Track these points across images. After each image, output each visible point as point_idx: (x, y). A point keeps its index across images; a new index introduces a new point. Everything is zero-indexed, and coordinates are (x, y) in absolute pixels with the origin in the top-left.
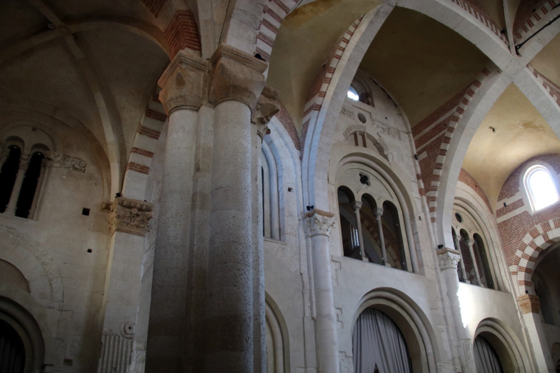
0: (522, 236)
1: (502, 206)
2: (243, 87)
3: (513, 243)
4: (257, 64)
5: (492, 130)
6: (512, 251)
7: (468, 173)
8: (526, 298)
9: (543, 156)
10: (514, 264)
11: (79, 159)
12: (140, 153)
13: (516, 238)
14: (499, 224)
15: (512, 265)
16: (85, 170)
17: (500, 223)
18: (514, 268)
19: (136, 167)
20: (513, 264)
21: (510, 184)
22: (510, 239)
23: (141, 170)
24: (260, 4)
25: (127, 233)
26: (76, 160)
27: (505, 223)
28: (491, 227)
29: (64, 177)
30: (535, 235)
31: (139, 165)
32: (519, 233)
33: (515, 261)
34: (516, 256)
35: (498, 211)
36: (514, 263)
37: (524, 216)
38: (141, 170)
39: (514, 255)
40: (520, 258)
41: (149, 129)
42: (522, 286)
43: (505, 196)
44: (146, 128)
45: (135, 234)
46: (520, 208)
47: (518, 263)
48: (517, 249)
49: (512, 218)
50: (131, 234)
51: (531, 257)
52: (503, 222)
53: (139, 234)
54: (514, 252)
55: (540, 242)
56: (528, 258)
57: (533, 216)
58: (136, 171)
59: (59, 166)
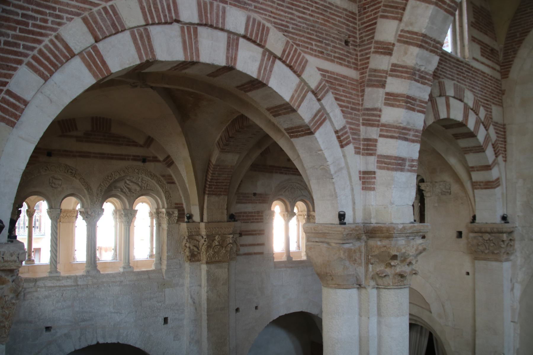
2: (323, 273)
4: (334, 233)
11: (444, 181)
12: (478, 170)
16: (450, 192)
19: (480, 185)
23: (486, 187)
24: (319, 151)
25: (484, 260)
26: (442, 183)
29: (436, 205)
31: (482, 182)
38: (486, 187)
41: (469, 148)
44: (466, 148)
45: (493, 261)
50: (489, 260)
53: (497, 260)
58: (482, 189)
59: (430, 195)
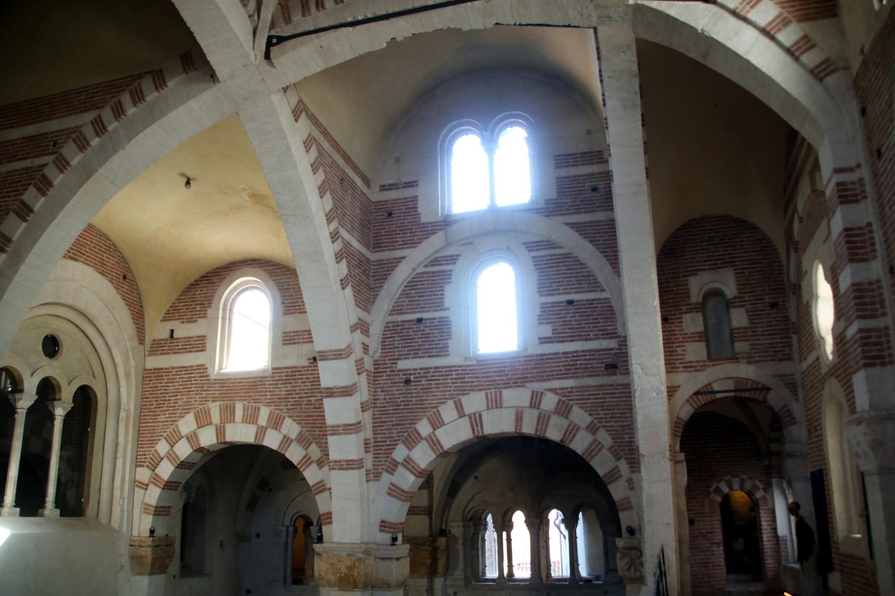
0: (180, 413)
1: (167, 335)
3: (159, 422)
5: (185, 180)
6: (152, 437)
7: (114, 245)
8: (147, 544)
9: (273, 266)
10: (147, 466)
13: (167, 412)
14: (147, 370)
15: (143, 466)
17: (151, 370)
18: (143, 474)
20: (145, 464)
21: (195, 294)
22: (156, 411)
27: (158, 372)
28: (128, 375)
30: (203, 420)
32: (176, 405)
33: (150, 460)
34: (156, 451)
35: (154, 340)
36: (147, 463)
37: (197, 373)
39: (154, 447)
40: (162, 459)
42: (147, 516)
43: (179, 316)
46: (196, 353)
47: (156, 467)
48: (162, 436)
49: (174, 368)
51: (156, 507)
52: (155, 369)
54: (155, 442)
55: (208, 438)
56: (176, 462)
57: (212, 381)
